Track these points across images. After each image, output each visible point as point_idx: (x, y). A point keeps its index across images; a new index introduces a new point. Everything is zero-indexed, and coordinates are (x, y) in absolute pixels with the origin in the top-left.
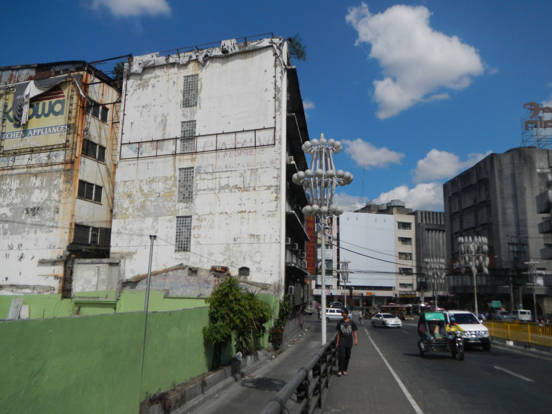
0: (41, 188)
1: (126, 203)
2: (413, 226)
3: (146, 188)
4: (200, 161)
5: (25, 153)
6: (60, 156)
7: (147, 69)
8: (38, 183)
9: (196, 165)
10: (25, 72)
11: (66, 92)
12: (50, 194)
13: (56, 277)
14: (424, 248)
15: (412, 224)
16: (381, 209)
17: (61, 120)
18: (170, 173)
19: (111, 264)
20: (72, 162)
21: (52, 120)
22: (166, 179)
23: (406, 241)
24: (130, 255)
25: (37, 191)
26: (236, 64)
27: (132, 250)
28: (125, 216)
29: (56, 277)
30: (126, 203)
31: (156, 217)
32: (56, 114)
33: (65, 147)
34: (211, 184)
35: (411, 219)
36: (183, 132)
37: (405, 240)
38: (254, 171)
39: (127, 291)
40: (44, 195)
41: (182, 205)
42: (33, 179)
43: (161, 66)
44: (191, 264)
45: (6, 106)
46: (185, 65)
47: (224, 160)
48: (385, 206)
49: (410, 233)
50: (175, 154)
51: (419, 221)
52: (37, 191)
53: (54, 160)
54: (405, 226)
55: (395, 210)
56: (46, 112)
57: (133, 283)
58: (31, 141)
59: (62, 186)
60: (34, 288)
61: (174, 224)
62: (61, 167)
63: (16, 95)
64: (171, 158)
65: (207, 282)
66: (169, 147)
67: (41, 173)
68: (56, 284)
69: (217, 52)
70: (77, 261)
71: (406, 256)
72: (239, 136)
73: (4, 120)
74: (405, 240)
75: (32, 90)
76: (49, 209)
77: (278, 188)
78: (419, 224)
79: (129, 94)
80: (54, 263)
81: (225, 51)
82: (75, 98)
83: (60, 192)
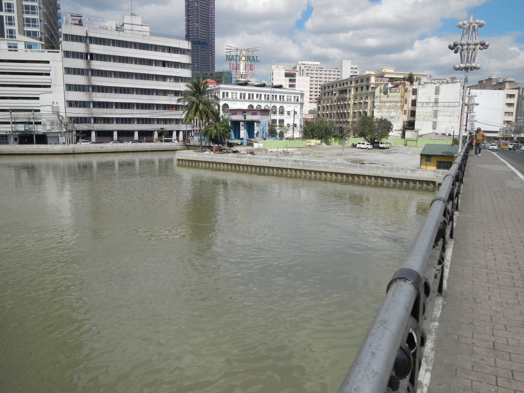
0: (394, 112)
1: (419, 117)
2: (516, 96)
3: (424, 114)
4: (439, 109)
5: (388, 102)
6: (399, 104)
7: (425, 83)
8: (393, 110)
9: (438, 109)
10: (386, 79)
11: (400, 86)
12: (397, 114)
13: (400, 134)
14: (521, 109)
15: (516, 95)
16: (499, 82)
17: (399, 94)
18: (431, 111)
19: (415, 132)
20: (403, 106)
21: (396, 94)
22: (430, 112)
23: (510, 105)
24: (420, 130)
25: (392, 113)
26: (450, 85)
27: (421, 128)
28: (419, 121)
29: (400, 134)
30: (419, 117)
31: (427, 121)
32: (397, 92)
33: (401, 102)
34: (442, 114)
35: (516, 92)
36: (435, 101)
37: (510, 105)
38: (453, 112)
39: (419, 138)
40: (395, 114)
41: (434, 119)
42: (391, 109)
43: (429, 83)
44: (436, 132)
45: (380, 88)
46: (436, 84)
47: (446, 109)
48: (502, 79)
49: (514, 101)
50: (432, 106)
51: (521, 94)
52: (392, 113)
53: (397, 105)
54: (511, 96)
55: (507, 85)
56: (394, 91)
57: (421, 136)
58: (390, 99)
59: (400, 112)
60: (393, 136)
61: (432, 123)
62: (400, 107)
63: (385, 86)
64: (431, 107)
65: (441, 136)
66: (431, 105)
67: (393, 108)
68: (400, 136)
69: (445, 81)
70: (406, 130)
71: (509, 114)
72: (450, 103)
73: (380, 93)
74: (510, 105)
75: (390, 85)
76: (397, 117)
77: (459, 116)
78: (520, 95)
79: (419, 89)
80: (399, 131)
81: (447, 82)
82: (403, 89)
83: (400, 113)
